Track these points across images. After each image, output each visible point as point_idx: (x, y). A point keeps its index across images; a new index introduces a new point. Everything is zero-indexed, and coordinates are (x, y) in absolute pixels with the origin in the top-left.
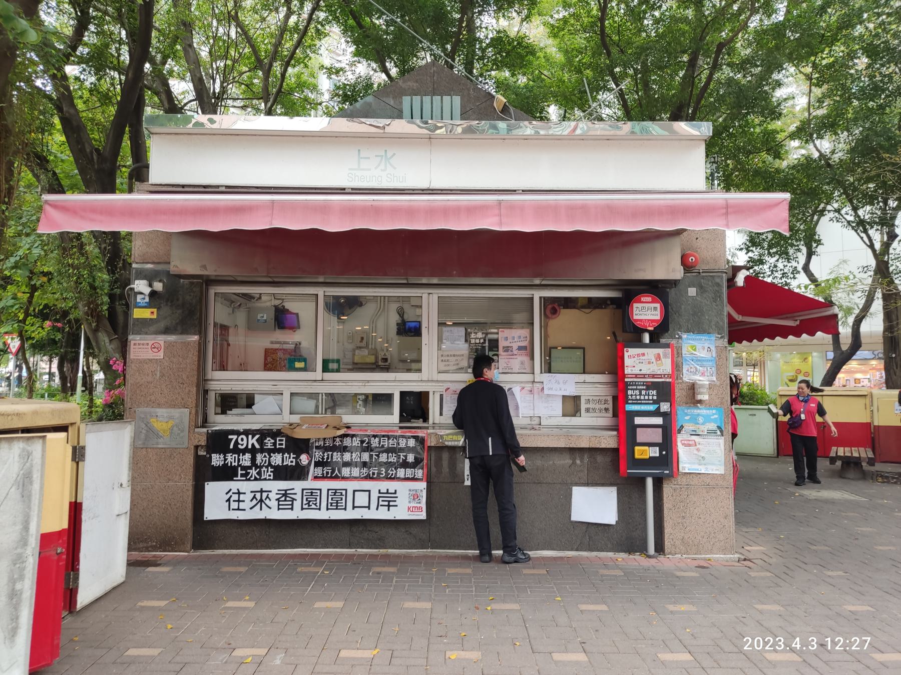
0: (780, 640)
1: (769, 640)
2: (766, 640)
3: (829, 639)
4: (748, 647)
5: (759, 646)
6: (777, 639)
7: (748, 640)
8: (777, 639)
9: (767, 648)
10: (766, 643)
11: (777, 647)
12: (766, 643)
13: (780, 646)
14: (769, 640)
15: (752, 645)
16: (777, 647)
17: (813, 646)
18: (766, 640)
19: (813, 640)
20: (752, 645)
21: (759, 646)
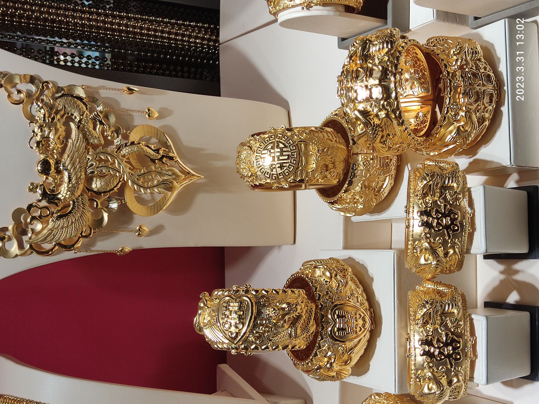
0: (518, 79)
1: (518, 85)
2: (518, 87)
3: (518, 43)
4: (522, 21)
5: (522, 92)
6: (518, 81)
7: (518, 98)
8: (518, 81)
9: (523, 87)
10: (520, 88)
11: (522, 81)
12: (520, 88)
13: (522, 79)
14: (518, 85)
15: (521, 96)
16: (522, 81)
17: (522, 59)
18: (518, 87)
19: (518, 69)
20: (521, 96)
21: (522, 92)
